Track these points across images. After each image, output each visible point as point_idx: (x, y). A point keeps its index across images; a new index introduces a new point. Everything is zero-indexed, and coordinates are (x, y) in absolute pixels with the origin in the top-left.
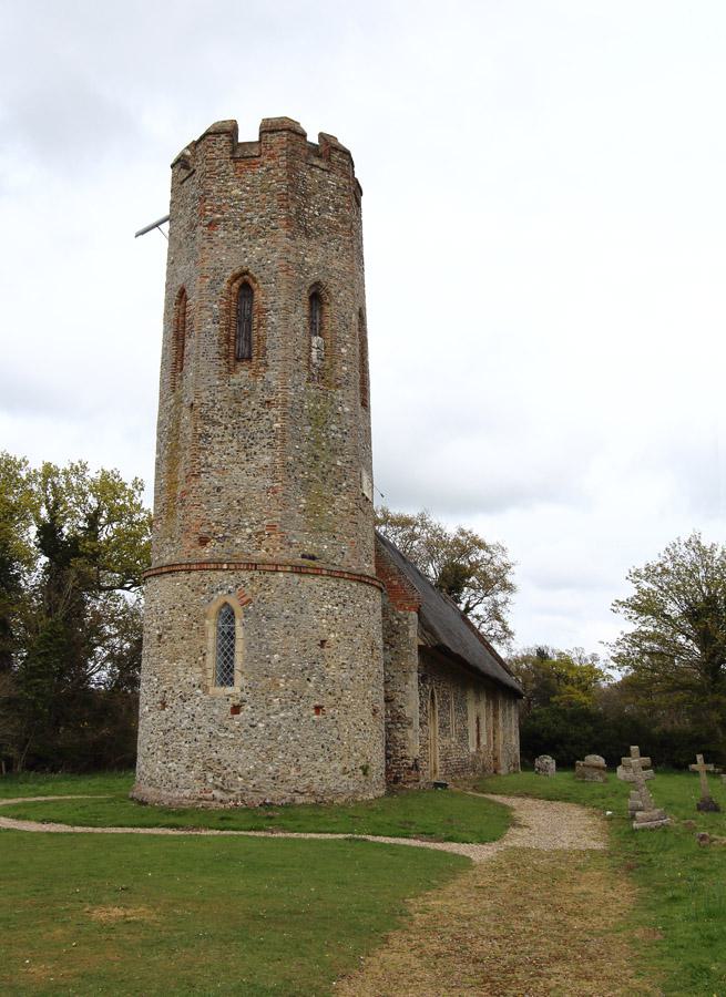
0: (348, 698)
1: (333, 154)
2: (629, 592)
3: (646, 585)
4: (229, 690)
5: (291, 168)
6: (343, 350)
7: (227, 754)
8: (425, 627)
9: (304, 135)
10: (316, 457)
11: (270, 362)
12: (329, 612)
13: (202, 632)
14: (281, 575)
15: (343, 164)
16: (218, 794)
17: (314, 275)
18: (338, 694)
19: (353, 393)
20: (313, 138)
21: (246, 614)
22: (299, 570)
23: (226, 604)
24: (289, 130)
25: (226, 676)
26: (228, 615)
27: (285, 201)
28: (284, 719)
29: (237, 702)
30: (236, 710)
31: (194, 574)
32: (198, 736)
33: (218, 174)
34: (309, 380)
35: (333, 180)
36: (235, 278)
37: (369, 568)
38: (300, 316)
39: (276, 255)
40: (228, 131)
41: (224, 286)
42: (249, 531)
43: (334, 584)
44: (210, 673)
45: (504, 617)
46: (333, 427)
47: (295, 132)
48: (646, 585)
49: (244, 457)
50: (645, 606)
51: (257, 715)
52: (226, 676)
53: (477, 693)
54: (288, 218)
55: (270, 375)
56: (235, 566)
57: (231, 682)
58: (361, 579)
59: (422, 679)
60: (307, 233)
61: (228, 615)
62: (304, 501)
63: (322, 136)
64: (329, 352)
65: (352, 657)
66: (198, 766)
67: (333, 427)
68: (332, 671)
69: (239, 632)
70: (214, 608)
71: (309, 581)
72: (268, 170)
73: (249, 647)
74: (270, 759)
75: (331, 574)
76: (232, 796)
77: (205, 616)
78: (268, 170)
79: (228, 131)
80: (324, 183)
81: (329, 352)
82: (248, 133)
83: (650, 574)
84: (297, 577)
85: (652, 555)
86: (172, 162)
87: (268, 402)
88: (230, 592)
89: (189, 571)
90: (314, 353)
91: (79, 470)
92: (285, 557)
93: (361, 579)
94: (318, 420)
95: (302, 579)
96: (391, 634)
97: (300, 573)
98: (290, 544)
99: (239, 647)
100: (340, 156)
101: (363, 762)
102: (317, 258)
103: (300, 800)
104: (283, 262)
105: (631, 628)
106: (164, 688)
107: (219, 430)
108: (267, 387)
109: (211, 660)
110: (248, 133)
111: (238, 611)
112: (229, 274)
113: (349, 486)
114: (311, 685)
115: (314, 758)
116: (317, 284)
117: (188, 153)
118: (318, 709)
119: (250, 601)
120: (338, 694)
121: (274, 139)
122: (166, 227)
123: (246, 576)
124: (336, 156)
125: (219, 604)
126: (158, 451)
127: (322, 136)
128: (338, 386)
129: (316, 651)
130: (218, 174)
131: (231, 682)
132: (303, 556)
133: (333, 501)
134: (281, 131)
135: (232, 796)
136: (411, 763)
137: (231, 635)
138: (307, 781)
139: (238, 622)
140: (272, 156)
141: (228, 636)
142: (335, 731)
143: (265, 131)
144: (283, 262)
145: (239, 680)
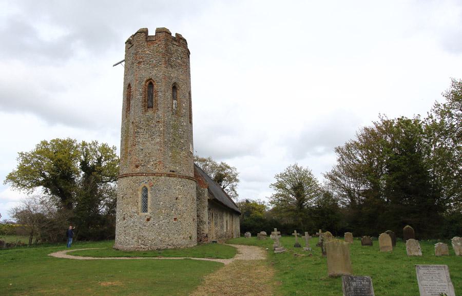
0: (185, 215)
1: (180, 41)
2: (275, 181)
3: (280, 179)
4: (146, 214)
5: (166, 45)
7: (145, 234)
8: (210, 193)
9: (171, 34)
11: (159, 108)
12: (179, 189)
13: (137, 195)
14: (163, 177)
16: (142, 246)
17: (174, 80)
18: (182, 214)
19: (187, 119)
20: (174, 35)
21: (152, 189)
22: (169, 175)
23: (145, 186)
24: (165, 32)
25: (145, 209)
26: (145, 190)
27: (164, 55)
28: (164, 222)
29: (148, 217)
30: (148, 220)
31: (134, 177)
32: (136, 228)
33: (141, 46)
35: (180, 49)
36: (147, 81)
37: (192, 175)
38: (169, 94)
39: (161, 73)
40: (144, 32)
41: (144, 83)
42: (152, 163)
43: (180, 180)
44: (140, 209)
45: (236, 190)
47: (167, 33)
48: (280, 179)
49: (150, 139)
50: (280, 186)
51: (155, 221)
52: (145, 209)
53: (227, 213)
54: (165, 61)
55: (159, 113)
56: (147, 174)
57: (146, 211)
58: (189, 178)
59: (209, 209)
60: (172, 66)
61: (145, 190)
63: (176, 34)
64: (179, 105)
65: (186, 203)
66: (136, 238)
68: (180, 207)
69: (149, 195)
70: (141, 188)
71: (172, 179)
72: (159, 45)
73: (152, 200)
74: (160, 235)
75: (179, 177)
76: (147, 247)
77: (138, 190)
78: (159, 45)
79: (144, 32)
80: (177, 50)
81: (179, 105)
82: (152, 33)
83: (282, 176)
84: (168, 178)
85: (282, 170)
86: (125, 41)
87: (159, 121)
88: (146, 183)
89: (132, 176)
90: (174, 106)
91: (95, 143)
92: (164, 171)
93: (189, 178)
94: (175, 127)
95: (170, 178)
96: (199, 195)
97: (169, 176)
99: (149, 200)
101: (190, 235)
102: (174, 74)
103: (169, 247)
104: (163, 76)
105: (275, 192)
106: (124, 213)
107: (142, 130)
108: (158, 117)
109: (140, 204)
110: (152, 33)
111: (149, 189)
112: (145, 79)
114: (173, 212)
115: (174, 235)
116: (175, 83)
117: (131, 39)
118: (175, 219)
119: (153, 185)
121: (160, 35)
122: (124, 63)
123: (151, 177)
124: (181, 41)
125: (143, 186)
126: (122, 137)
127: (176, 34)
128: (182, 117)
129: (175, 201)
130: (141, 46)
131: (146, 211)
132: (170, 171)
133: (180, 153)
134: (163, 32)
135: (147, 247)
136: (205, 235)
137: (146, 196)
138: (172, 242)
139: (149, 192)
140: (160, 41)
141: (145, 197)
142: (181, 226)
144: (163, 76)
145: (149, 210)
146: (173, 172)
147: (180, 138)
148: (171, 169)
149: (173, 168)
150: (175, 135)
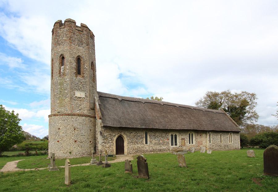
0: (65, 139)
6: (67, 67)
10: (61, 92)
12: (61, 123)
15: (68, 24)
17: (60, 54)
18: (62, 138)
34: (60, 76)
43: (61, 117)
46: (65, 84)
62: (58, 101)
64: (64, 70)
67: (65, 84)
68: (61, 134)
71: (56, 117)
75: (60, 115)
98: (55, 110)
100: (68, 22)
101: (70, 151)
113: (68, 96)
114: (57, 137)
116: (62, 55)
120: (62, 138)
129: (58, 130)
133: (65, 100)
143: (66, 22)
146: (59, 112)
147: (65, 90)
148: (58, 111)
149: (59, 110)
150: (61, 89)
